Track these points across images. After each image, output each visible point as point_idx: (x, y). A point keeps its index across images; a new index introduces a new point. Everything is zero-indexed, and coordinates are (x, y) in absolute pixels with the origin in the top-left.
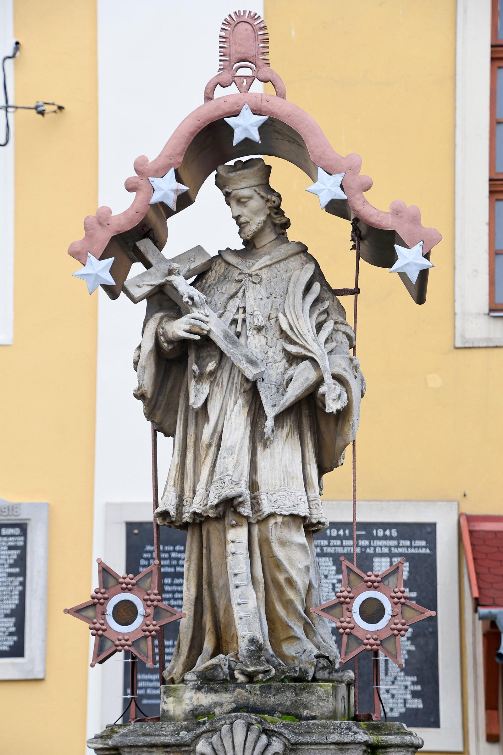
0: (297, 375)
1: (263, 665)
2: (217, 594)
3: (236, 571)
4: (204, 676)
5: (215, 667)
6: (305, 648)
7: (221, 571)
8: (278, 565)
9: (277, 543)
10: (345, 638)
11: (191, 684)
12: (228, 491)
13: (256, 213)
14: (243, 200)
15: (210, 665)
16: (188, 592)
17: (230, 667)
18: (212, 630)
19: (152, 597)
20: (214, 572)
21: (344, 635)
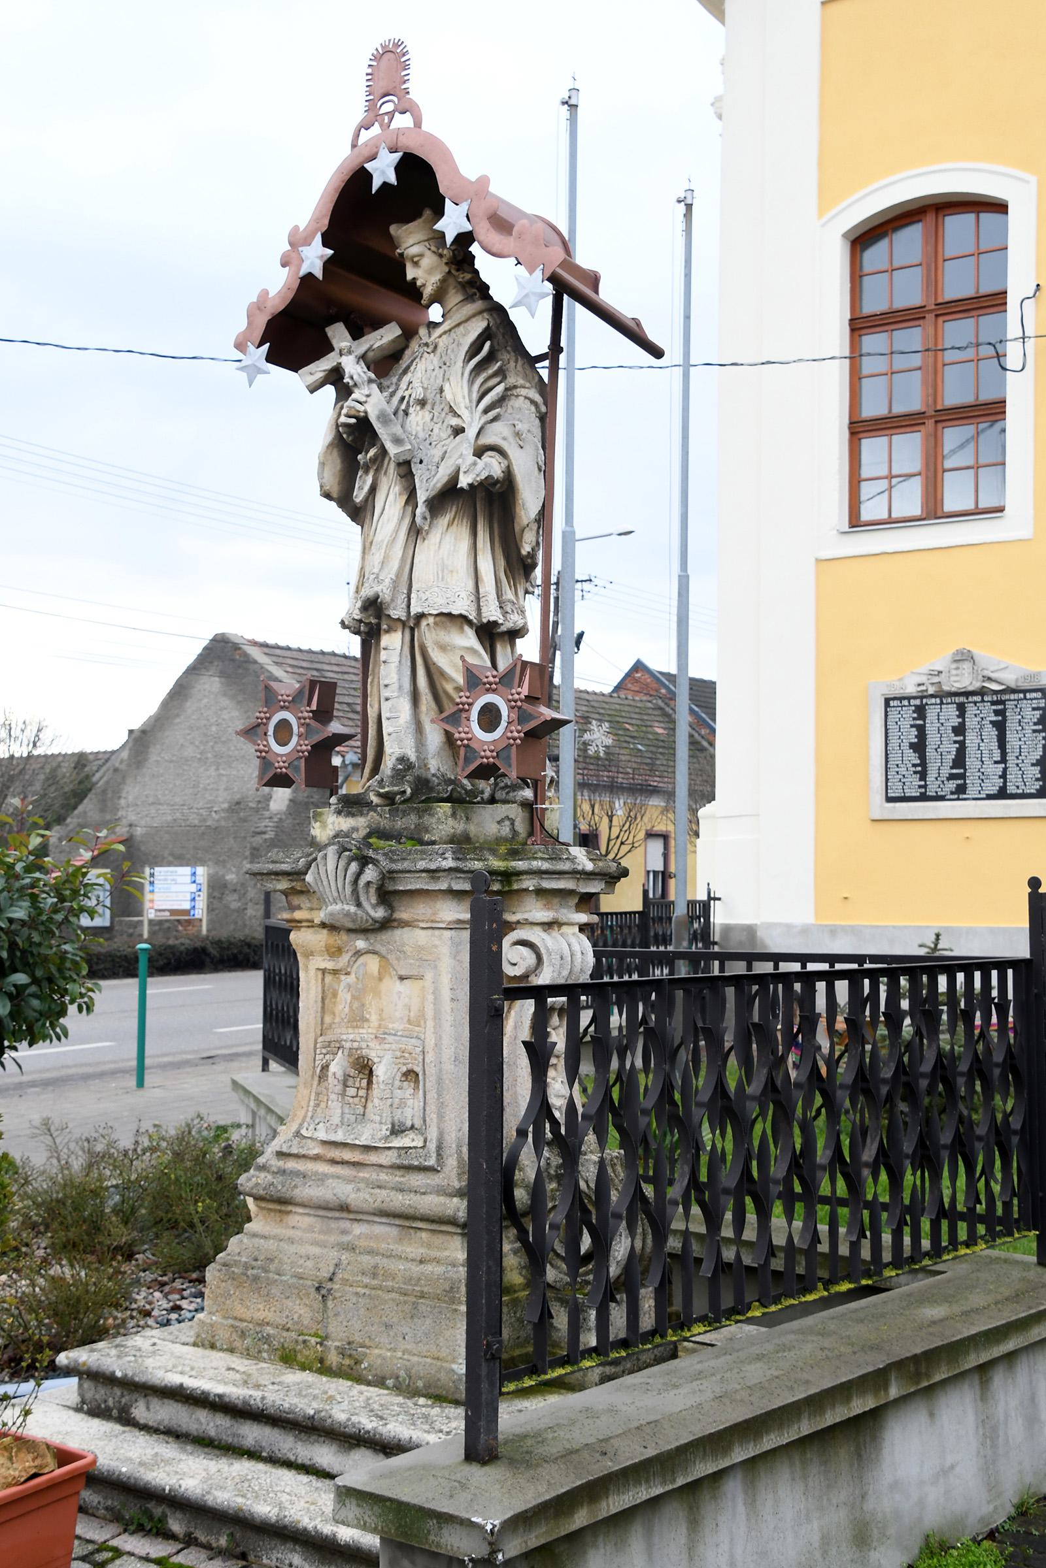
3: (386, 682)
10: (462, 751)
11: (333, 807)
13: (430, 272)
14: (416, 259)
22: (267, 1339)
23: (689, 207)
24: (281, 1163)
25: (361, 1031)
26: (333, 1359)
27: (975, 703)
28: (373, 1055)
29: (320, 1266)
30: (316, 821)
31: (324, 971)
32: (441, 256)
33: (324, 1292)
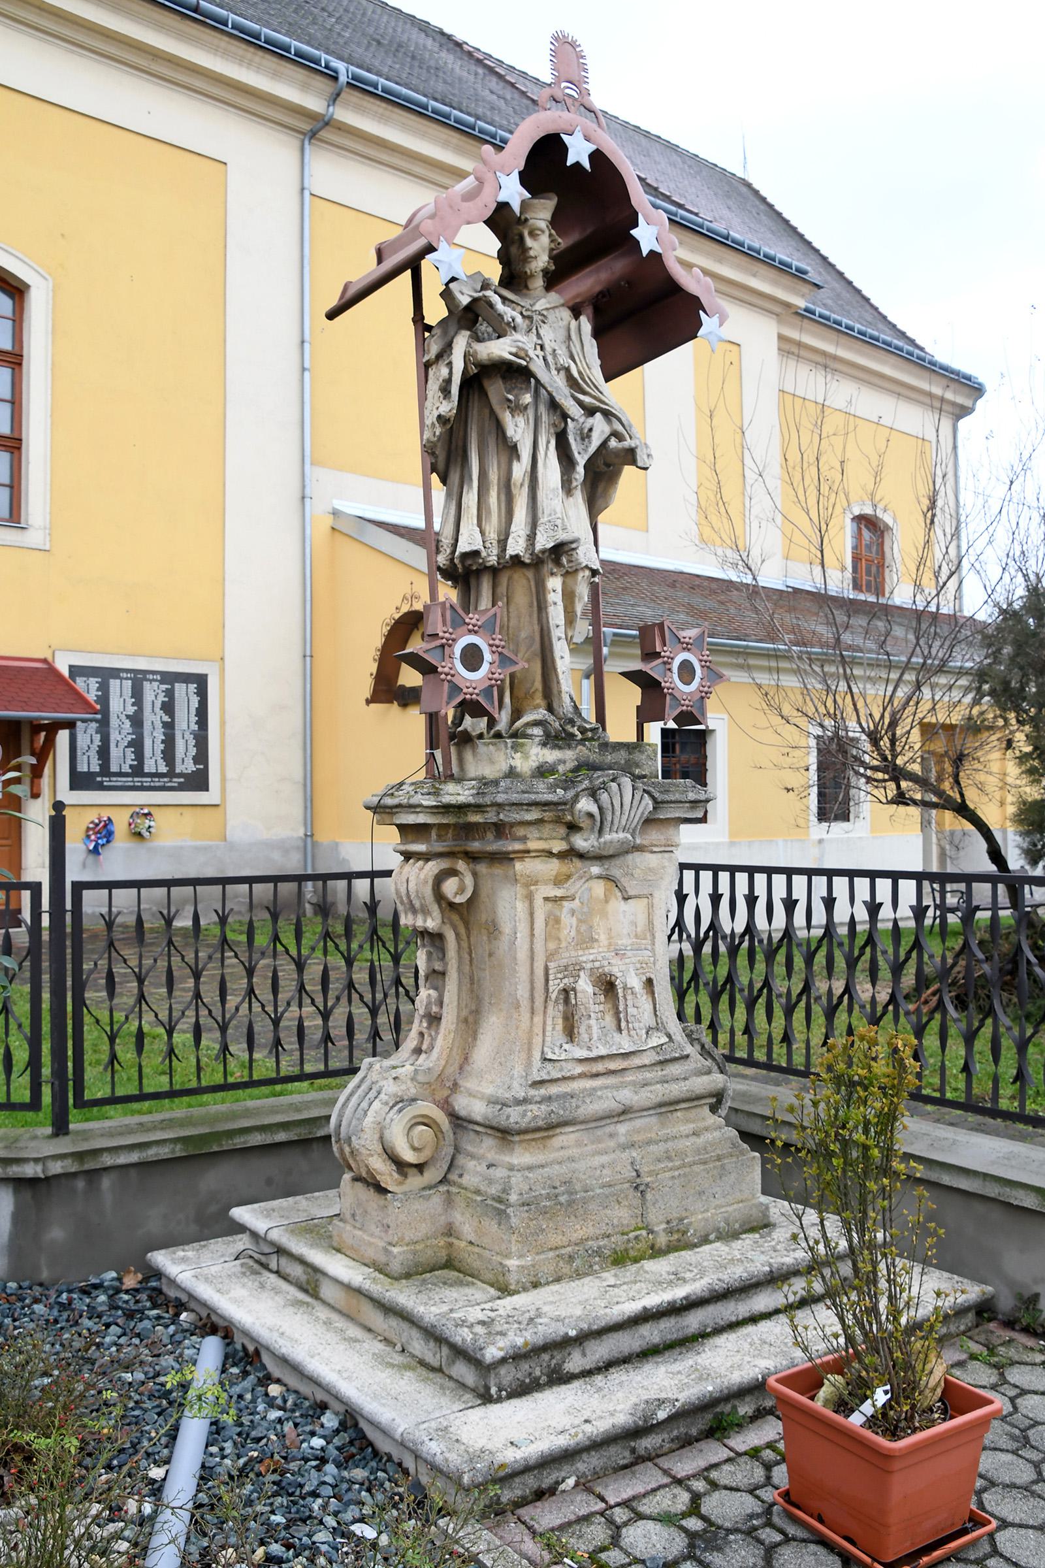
19: (497, 642)
22: (598, 1252)
24: (543, 1091)
25: (591, 951)
26: (662, 1240)
28: (615, 970)
29: (618, 1169)
30: (516, 752)
31: (546, 899)
33: (642, 1188)
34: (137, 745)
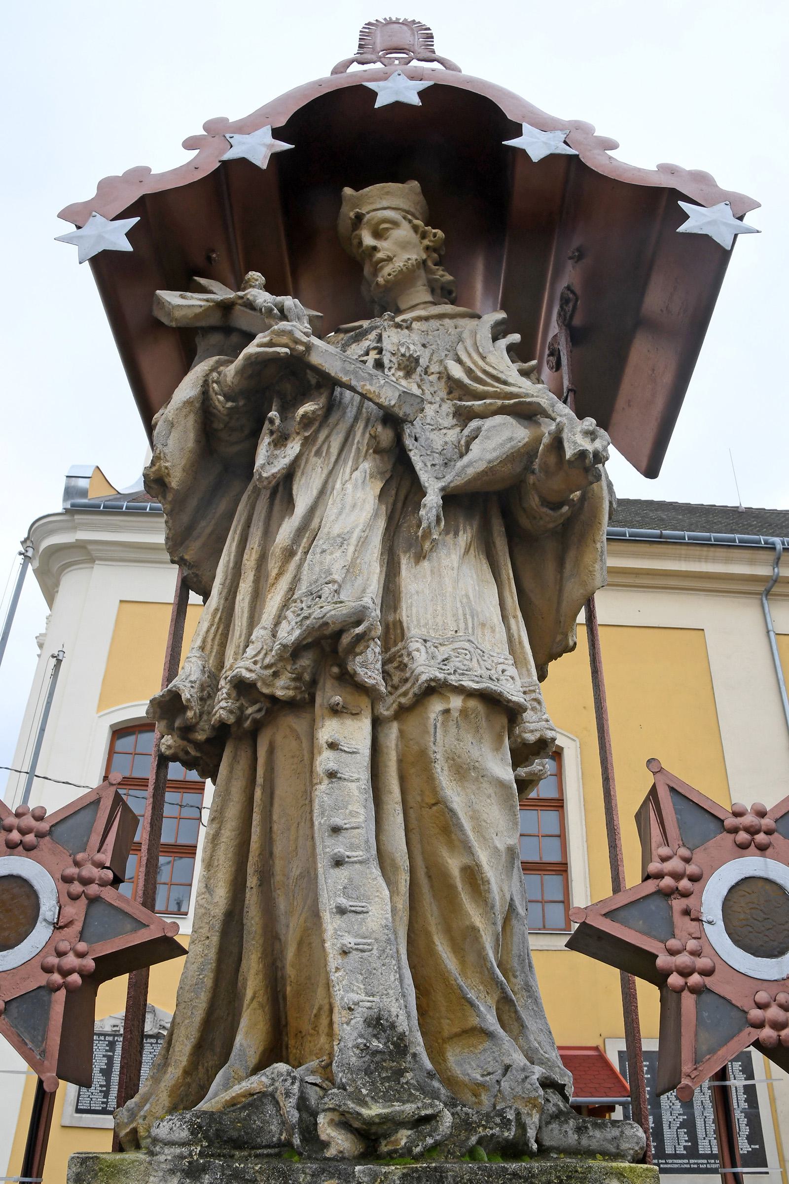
0: (488, 430)
1: (411, 1099)
2: (282, 904)
3: (338, 821)
4: (214, 1127)
5: (256, 1101)
6: (507, 1061)
7: (297, 839)
8: (449, 827)
9: (446, 768)
11: (169, 1153)
12: (327, 608)
13: (404, 245)
15: (244, 1095)
16: (207, 896)
17: (302, 1104)
18: (262, 998)
19: (89, 871)
20: (278, 849)
21: (686, 994)
23: (59, 662)
27: (151, 1044)
32: (424, 236)
34: (689, 1125)
